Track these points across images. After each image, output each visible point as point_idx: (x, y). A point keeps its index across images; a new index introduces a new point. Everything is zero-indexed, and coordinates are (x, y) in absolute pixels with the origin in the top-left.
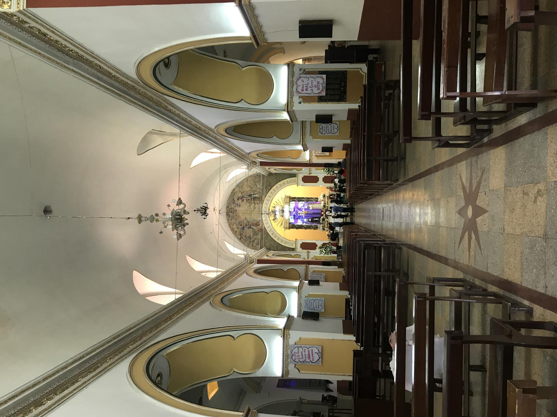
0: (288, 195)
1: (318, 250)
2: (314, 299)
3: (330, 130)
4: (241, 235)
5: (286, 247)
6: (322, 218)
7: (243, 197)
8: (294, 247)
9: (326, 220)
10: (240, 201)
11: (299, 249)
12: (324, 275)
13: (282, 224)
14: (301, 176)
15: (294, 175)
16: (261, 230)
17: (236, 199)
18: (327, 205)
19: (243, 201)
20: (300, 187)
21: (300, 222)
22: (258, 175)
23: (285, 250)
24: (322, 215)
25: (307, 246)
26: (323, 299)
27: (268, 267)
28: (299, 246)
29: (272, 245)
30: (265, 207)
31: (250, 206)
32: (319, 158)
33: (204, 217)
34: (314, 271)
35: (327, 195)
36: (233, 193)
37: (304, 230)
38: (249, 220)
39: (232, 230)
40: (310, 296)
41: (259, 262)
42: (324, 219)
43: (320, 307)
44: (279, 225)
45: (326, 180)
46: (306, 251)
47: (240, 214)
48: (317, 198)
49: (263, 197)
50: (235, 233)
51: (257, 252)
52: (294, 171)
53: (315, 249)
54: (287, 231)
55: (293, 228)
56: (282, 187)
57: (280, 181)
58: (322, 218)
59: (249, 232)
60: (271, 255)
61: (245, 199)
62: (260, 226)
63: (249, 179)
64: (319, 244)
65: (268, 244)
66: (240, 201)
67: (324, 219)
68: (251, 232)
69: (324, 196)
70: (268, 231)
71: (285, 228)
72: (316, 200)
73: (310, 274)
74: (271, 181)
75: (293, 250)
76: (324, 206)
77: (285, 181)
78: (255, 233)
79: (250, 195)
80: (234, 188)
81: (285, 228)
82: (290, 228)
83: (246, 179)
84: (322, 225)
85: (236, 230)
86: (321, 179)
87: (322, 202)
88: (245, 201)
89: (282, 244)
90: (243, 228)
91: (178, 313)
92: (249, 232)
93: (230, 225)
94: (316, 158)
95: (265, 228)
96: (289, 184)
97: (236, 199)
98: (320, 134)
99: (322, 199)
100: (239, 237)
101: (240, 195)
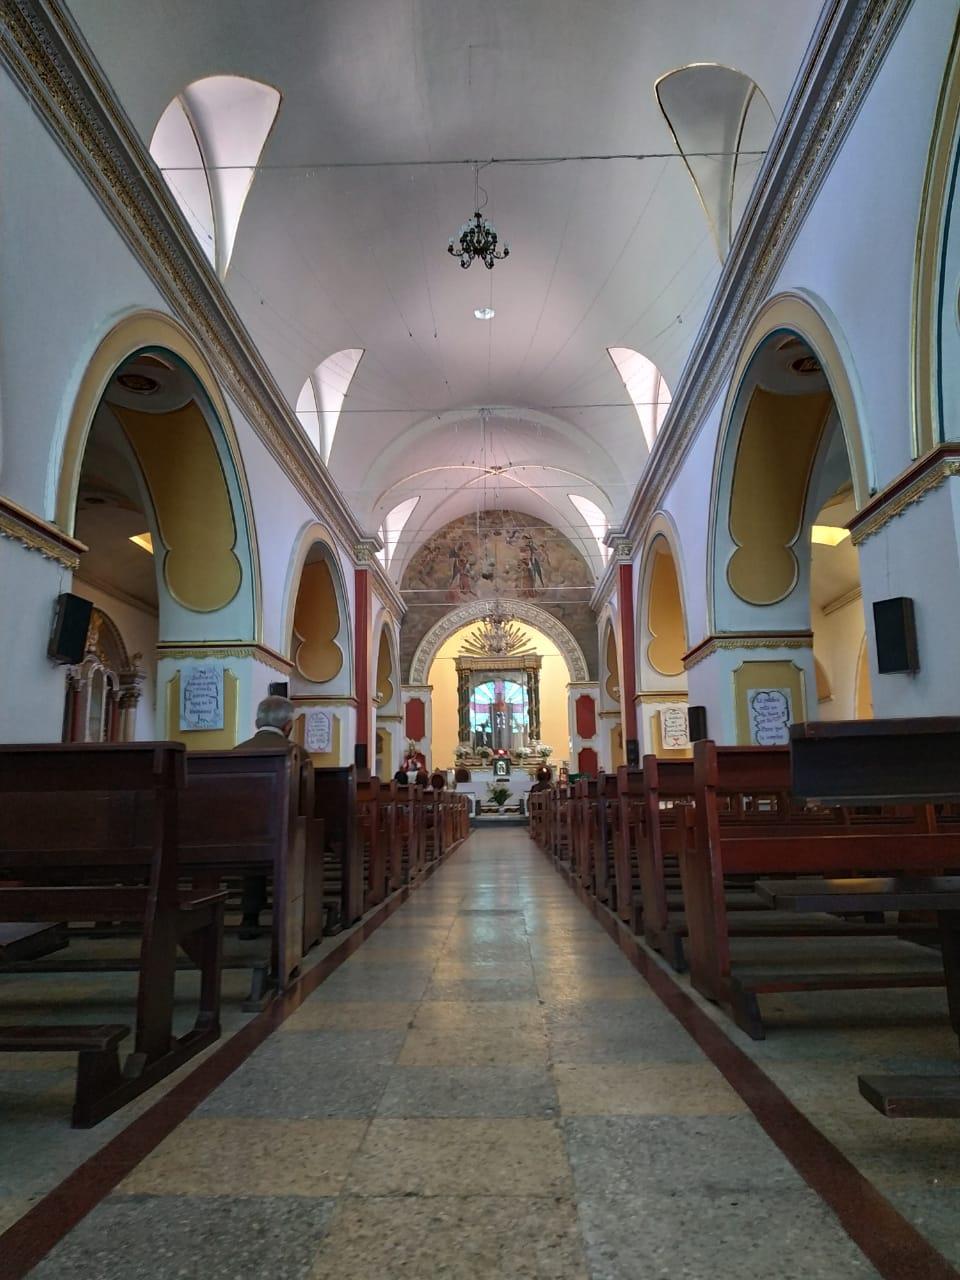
0: (544, 662)
2: (221, 698)
3: (767, 725)
6: (490, 751)
7: (532, 549)
8: (411, 682)
9: (484, 761)
10: (522, 543)
11: (406, 696)
12: (329, 749)
13: (468, 650)
14: (595, 693)
15: (594, 675)
16: (452, 597)
18: (522, 761)
19: (523, 550)
20: (566, 693)
22: (586, 576)
24: (496, 752)
25: (416, 719)
26: (220, 725)
27: (342, 586)
28: (414, 694)
29: (414, 627)
30: (509, 605)
32: (654, 721)
33: (458, 247)
34: (336, 720)
35: (550, 761)
36: (538, 522)
37: (457, 706)
39: (451, 526)
40: (229, 682)
41: (361, 576)
42: (485, 755)
43: (194, 718)
44: (467, 645)
45: (587, 757)
46: (403, 713)
48: (538, 738)
49: (535, 601)
51: (397, 588)
52: (604, 674)
54: (453, 664)
55: (461, 678)
56: (561, 644)
57: (578, 640)
58: (490, 751)
59: (445, 568)
60: (386, 617)
61: (526, 555)
63: (578, 563)
64: (421, 747)
65: (416, 617)
67: (485, 755)
68: (444, 569)
69: (545, 754)
70: (448, 616)
71: (458, 660)
72: (534, 734)
73: (331, 710)
74: (577, 620)
75: (405, 680)
76: (519, 756)
77: (579, 653)
78: (442, 584)
79: (537, 564)
81: (458, 660)
82: (459, 670)
83: (577, 557)
84: (470, 751)
86: (587, 744)
87: (528, 751)
89: (418, 654)
90: (453, 554)
91: (110, 169)
92: (445, 568)
93: (461, 521)
94: (653, 713)
95: (455, 607)
96: (572, 663)
98: (751, 693)
99: (539, 748)
100: (433, 546)
101: (537, 542)
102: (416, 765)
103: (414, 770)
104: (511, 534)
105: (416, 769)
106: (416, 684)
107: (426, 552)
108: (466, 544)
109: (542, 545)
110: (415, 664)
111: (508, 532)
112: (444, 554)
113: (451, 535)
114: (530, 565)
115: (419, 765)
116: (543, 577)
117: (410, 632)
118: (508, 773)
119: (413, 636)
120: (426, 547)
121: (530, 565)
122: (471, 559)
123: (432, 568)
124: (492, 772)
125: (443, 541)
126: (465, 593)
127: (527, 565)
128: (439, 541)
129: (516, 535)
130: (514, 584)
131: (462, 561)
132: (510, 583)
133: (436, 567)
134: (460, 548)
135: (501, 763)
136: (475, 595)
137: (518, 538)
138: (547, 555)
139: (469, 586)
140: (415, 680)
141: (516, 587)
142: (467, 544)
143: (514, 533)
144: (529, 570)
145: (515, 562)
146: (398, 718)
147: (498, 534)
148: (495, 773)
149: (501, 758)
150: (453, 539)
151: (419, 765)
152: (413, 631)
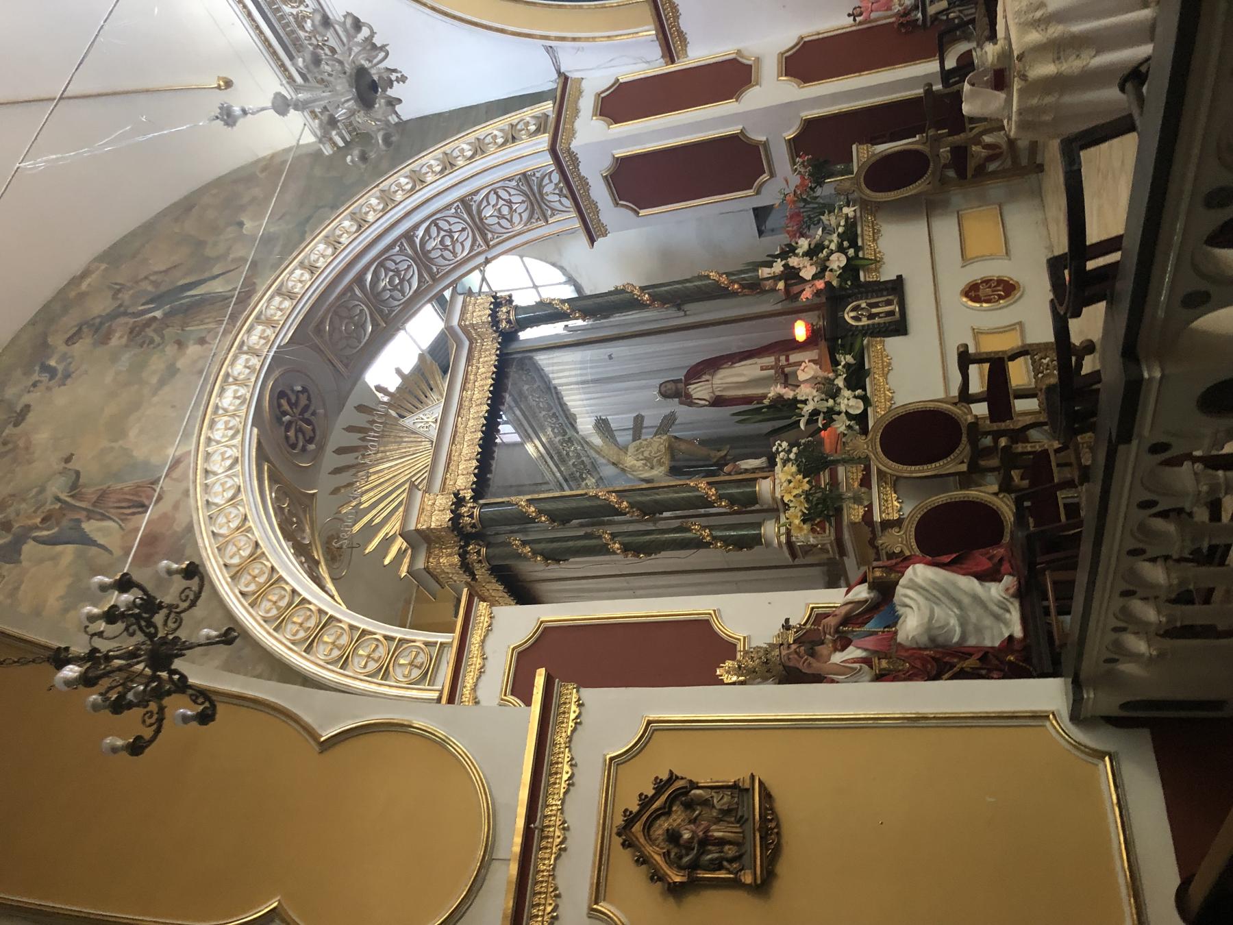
80: (77, 267)
86: (770, 69)
104: (45, 377)
114: (158, 314)
116: (207, 275)
121: (158, 314)
124: (893, 344)
131: (44, 520)
132: (179, 365)
135: (848, 316)
138: (146, 278)
139: (137, 490)
140: (427, 676)
141: (202, 341)
143: (46, 369)
144: (166, 315)
148: (899, 327)
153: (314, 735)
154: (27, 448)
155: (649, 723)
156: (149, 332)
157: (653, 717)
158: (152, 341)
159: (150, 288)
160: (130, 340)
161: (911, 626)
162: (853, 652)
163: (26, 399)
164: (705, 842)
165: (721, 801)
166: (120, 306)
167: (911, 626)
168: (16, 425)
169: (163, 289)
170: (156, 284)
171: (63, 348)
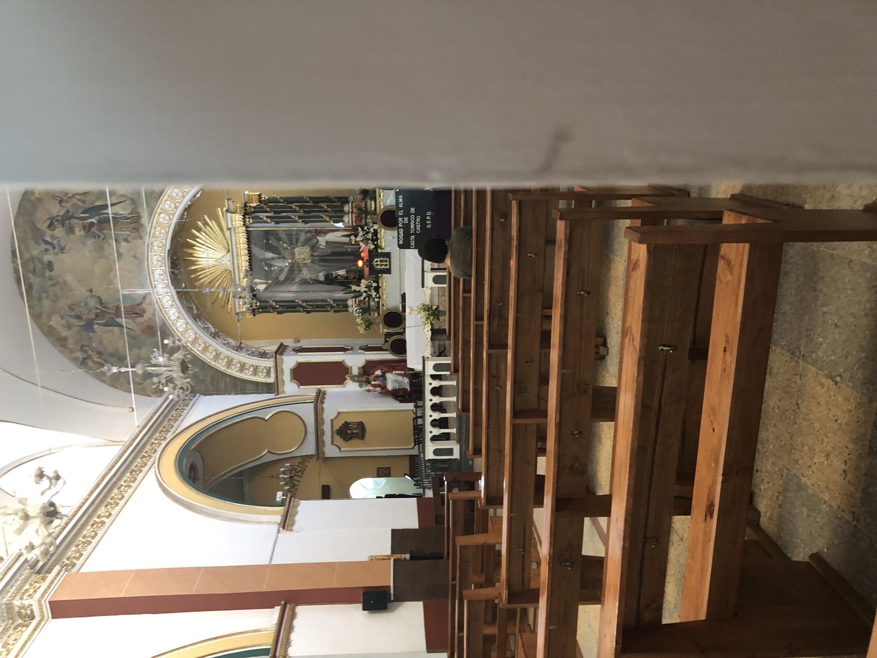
1: (351, 386)
4: (82, 348)
5: (244, 381)
8: (271, 380)
10: (59, 232)
11: (290, 388)
17: (44, 226)
19: (71, 230)
21: (288, 293)
23: (244, 392)
28: (287, 376)
31: (100, 249)
38: (105, 297)
39: (50, 333)
46: (311, 391)
47: (69, 278)
50: (61, 342)
53: (340, 381)
62: (147, 316)
66: (59, 232)
75: (269, 388)
85: (64, 333)
88: (79, 232)
89: (234, 372)
90: (89, 326)
93: (37, 317)
97: (44, 226)
100: (80, 355)
102: (378, 377)
103: (386, 379)
105: (383, 376)
106: (273, 375)
107: (90, 363)
108: (72, 309)
109: (61, 202)
110: (247, 376)
111: (46, 250)
112: (90, 339)
113: (59, 328)
114: (93, 220)
115: (378, 372)
117: (204, 382)
118: (388, 255)
119: (209, 379)
120: (83, 363)
121: (93, 220)
122: (92, 303)
123: (112, 355)
125: (70, 341)
126: (144, 312)
127: (92, 224)
128: (71, 343)
129: (48, 239)
130: (124, 244)
131: (97, 316)
133: (110, 350)
134: (79, 317)
136: (144, 297)
137: (52, 237)
140: (268, 374)
141: (126, 240)
142: (71, 308)
143: (46, 242)
145: (90, 242)
146: (320, 397)
147: (50, 266)
148: (388, 271)
149: (369, 263)
150: (69, 327)
151: (378, 372)
152: (201, 377)
153: (264, 419)
154: (65, 283)
155: (339, 413)
156: (94, 229)
157: (340, 410)
158: (99, 237)
159: (79, 203)
160: (87, 233)
161: (390, 387)
162: (376, 383)
163: (47, 258)
164: (352, 433)
165: (355, 427)
166: (68, 211)
167: (390, 387)
168: (51, 271)
169: (88, 205)
170: (84, 202)
171: (48, 231)
